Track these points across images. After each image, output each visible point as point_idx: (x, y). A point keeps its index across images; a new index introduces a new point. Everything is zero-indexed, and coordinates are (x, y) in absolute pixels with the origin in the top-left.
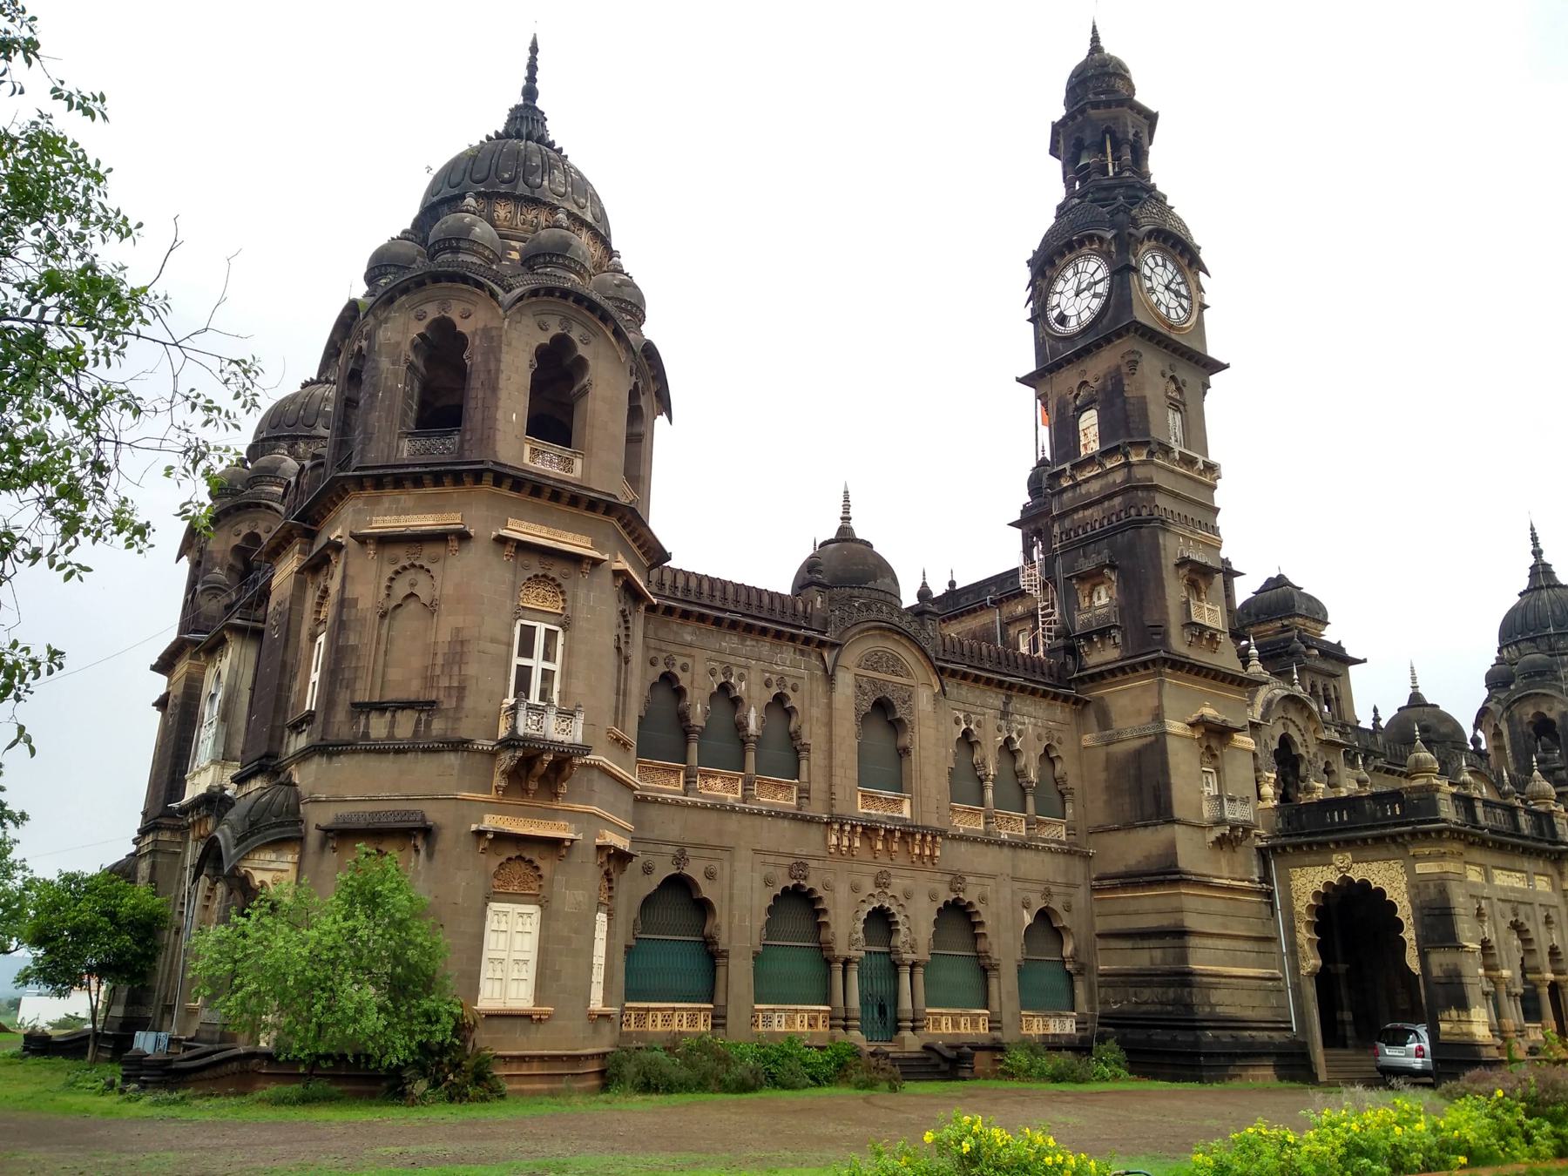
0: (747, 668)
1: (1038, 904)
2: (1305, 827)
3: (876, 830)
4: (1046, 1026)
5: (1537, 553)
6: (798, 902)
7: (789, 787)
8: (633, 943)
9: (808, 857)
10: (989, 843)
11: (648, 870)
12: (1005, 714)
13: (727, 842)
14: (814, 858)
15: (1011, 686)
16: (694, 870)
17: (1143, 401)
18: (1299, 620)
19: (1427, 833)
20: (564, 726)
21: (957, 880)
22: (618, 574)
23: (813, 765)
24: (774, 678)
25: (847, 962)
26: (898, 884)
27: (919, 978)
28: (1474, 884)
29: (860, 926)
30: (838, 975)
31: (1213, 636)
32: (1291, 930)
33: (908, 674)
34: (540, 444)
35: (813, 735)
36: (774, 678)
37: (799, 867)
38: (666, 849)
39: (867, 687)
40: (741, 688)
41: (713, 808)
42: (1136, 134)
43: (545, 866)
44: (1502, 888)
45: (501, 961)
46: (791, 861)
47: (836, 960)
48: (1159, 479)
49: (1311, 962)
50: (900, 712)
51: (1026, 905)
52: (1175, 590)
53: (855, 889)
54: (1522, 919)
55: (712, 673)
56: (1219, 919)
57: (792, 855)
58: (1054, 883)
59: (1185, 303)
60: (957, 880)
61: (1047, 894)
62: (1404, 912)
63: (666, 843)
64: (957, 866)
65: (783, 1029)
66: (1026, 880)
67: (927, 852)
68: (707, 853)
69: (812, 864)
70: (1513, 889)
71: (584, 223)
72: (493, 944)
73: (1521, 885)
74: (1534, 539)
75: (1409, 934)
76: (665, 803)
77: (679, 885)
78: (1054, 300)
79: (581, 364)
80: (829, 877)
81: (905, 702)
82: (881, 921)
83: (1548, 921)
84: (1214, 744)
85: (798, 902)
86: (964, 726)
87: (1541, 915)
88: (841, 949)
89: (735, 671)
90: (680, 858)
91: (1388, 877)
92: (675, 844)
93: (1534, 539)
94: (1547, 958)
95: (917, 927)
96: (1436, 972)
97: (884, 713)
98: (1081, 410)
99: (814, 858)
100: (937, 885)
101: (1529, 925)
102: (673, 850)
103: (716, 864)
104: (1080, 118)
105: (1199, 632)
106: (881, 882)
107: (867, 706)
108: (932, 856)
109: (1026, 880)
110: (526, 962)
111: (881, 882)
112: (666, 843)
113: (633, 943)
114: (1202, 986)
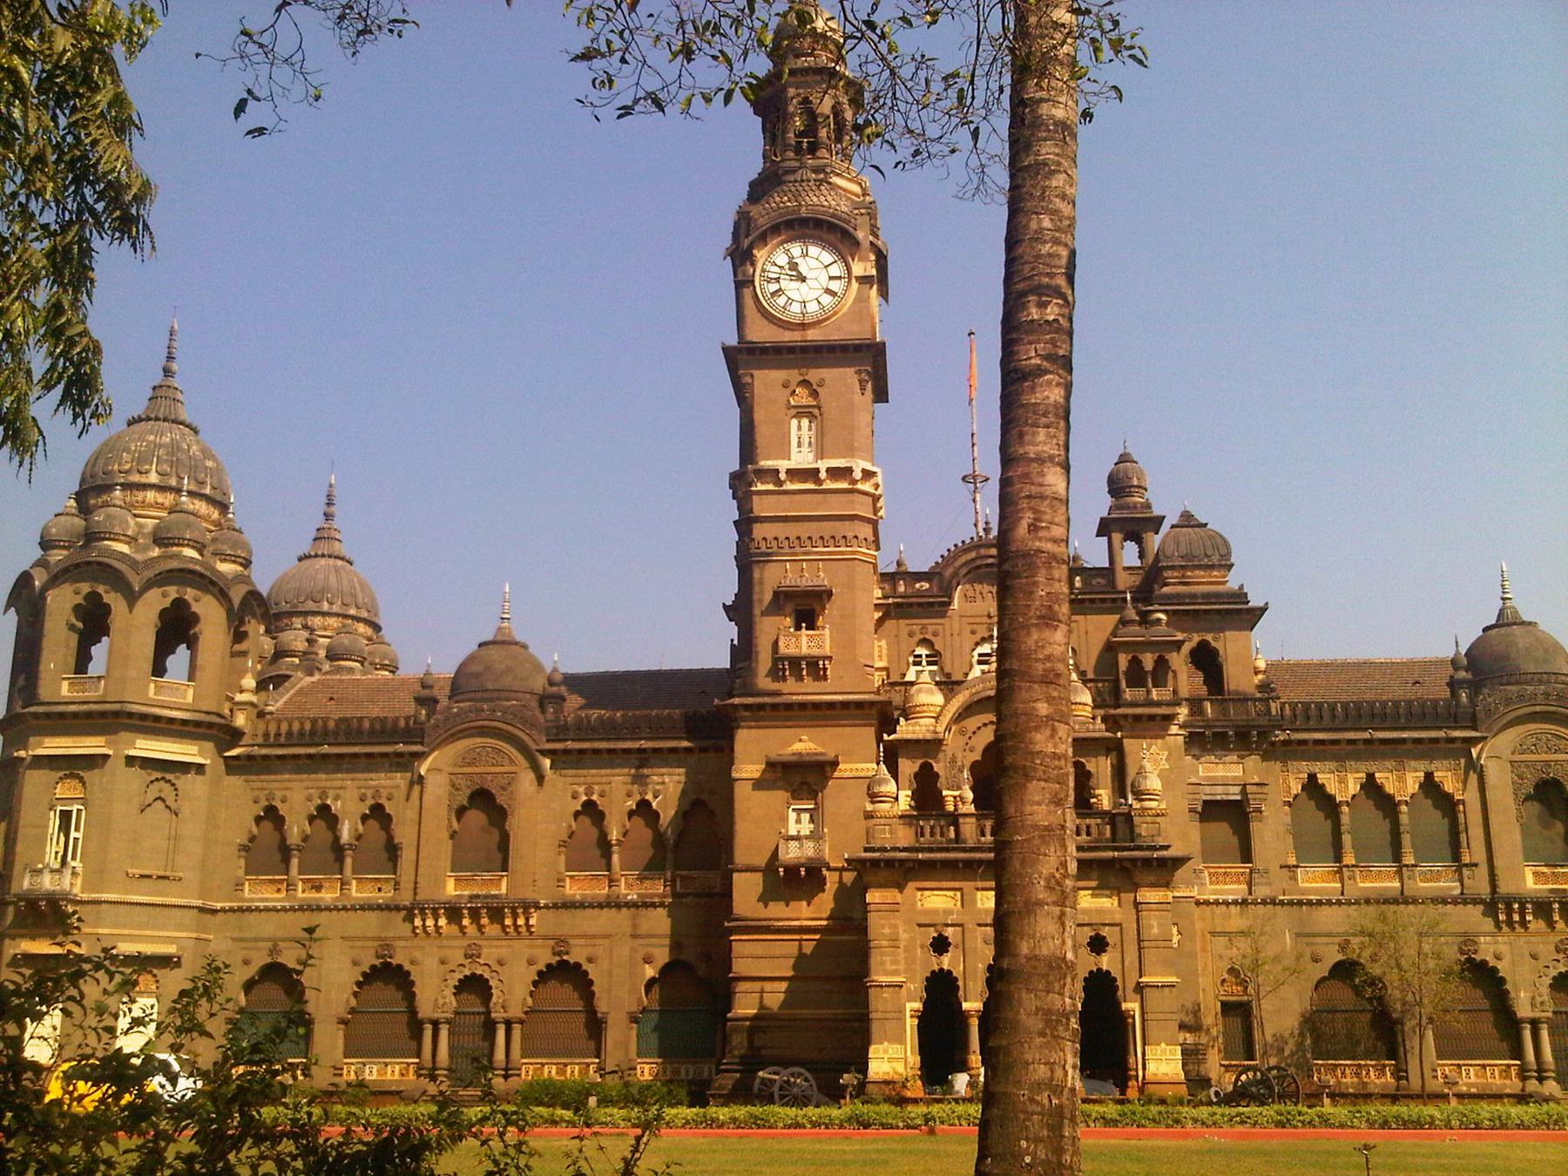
6: (388, 975)
9: (394, 938)
14: (401, 938)
15: (641, 751)
24: (369, 793)
26: (489, 953)
35: (404, 834)
37: (386, 947)
38: (261, 944)
39: (462, 782)
40: (336, 807)
41: (301, 909)
46: (376, 944)
50: (501, 800)
51: (648, 960)
53: (443, 962)
55: (309, 799)
57: (379, 939)
60: (561, 944)
64: (564, 931)
65: (374, 1077)
76: (258, 909)
80: (417, 954)
82: (474, 986)
84: (810, 780)
85: (388, 975)
89: (331, 793)
90: (274, 951)
92: (269, 940)
95: (513, 990)
97: (485, 803)
99: (401, 938)
107: (462, 799)
108: (528, 926)
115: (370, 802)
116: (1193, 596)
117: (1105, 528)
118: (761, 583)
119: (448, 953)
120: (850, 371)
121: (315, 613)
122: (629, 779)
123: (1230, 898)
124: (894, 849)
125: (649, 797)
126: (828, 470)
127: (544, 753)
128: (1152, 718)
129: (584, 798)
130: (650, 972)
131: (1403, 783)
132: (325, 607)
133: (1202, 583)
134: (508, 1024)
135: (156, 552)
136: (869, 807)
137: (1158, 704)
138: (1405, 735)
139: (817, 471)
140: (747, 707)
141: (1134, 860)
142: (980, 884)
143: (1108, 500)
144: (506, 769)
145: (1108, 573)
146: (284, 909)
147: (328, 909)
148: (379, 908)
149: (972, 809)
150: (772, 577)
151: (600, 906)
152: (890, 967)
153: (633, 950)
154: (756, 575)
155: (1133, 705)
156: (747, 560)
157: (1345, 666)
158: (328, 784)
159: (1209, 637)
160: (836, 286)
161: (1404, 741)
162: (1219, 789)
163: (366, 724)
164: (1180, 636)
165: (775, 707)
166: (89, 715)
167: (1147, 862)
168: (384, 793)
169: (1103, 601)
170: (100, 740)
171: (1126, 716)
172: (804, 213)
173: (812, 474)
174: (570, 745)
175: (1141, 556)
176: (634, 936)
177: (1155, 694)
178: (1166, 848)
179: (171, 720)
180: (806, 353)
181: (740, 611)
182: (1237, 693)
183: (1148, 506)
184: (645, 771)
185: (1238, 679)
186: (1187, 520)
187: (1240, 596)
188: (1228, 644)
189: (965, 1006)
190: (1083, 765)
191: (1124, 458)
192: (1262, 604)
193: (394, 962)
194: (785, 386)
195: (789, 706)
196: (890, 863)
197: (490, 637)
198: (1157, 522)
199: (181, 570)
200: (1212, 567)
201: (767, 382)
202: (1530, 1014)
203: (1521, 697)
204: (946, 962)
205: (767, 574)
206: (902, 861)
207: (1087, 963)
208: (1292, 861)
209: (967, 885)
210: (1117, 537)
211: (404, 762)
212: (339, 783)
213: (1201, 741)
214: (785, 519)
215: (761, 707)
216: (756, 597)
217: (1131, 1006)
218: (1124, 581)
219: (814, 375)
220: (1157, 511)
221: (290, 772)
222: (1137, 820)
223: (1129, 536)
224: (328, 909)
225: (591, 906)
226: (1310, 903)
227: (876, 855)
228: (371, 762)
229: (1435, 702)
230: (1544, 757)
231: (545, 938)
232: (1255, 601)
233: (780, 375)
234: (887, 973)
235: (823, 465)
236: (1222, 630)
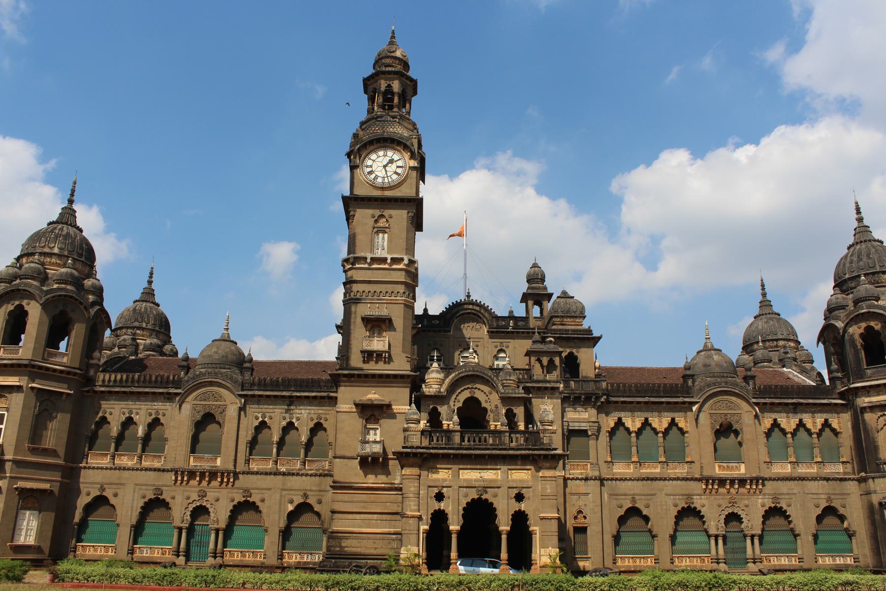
4: (303, 558)
7: (160, 457)
10: (275, 474)
11: (88, 494)
12: (287, 411)
13: (123, 481)
16: (108, 493)
24: (153, 412)
26: (211, 495)
30: (713, 542)
36: (153, 412)
37: (159, 491)
40: (136, 418)
51: (291, 502)
56: (362, 504)
58: (311, 490)
60: (247, 492)
61: (306, 496)
63: (96, 483)
64: (248, 485)
69: (164, 488)
76: (94, 468)
81: (221, 413)
84: (376, 413)
89: (134, 411)
90: (102, 489)
102: (99, 486)
103: (118, 491)
106: (203, 495)
111: (203, 495)
112: (96, 483)
115: (154, 416)
116: (566, 330)
117: (525, 298)
118: (355, 313)
120: (405, 212)
121: (139, 328)
122: (284, 411)
123: (580, 477)
124: (418, 447)
125: (294, 420)
126: (392, 259)
127: (240, 396)
128: (546, 388)
129: (261, 419)
130: (291, 508)
131: (660, 422)
132: (144, 325)
133: (570, 325)
134: (217, 531)
135: (55, 286)
136: (406, 426)
137: (549, 382)
138: (663, 400)
139: (386, 259)
140: (345, 375)
141: (539, 455)
142: (461, 467)
143: (527, 285)
145: (526, 319)
146: (107, 469)
147: (129, 469)
148: (155, 470)
149: (458, 428)
150: (364, 310)
151: (266, 474)
152: (413, 508)
153: (281, 496)
154: (353, 309)
155: (538, 381)
156: (349, 302)
157: (631, 370)
158: (133, 407)
159: (574, 351)
160: (399, 171)
161: (662, 403)
162: (576, 424)
164: (561, 349)
165: (359, 376)
166: (12, 365)
167: (546, 456)
168: (161, 412)
169: (523, 333)
170: (16, 379)
171: (533, 387)
172: (386, 135)
173: (383, 260)
174: (257, 393)
175: (541, 312)
177: (548, 377)
178: (556, 449)
179: (55, 370)
180: (382, 201)
181: (344, 328)
182: (586, 377)
183: (545, 288)
185: (586, 370)
186: (565, 295)
187: (589, 331)
188: (583, 354)
189: (451, 528)
190: (512, 410)
191: (535, 266)
192: (599, 335)
193: (161, 497)
194: (373, 217)
195: (366, 376)
196: (415, 455)
197: (218, 337)
198: (550, 296)
199: (65, 296)
200: (576, 317)
201: (364, 216)
202: (716, 533)
203: (714, 384)
204: (442, 505)
205: (358, 309)
206: (422, 454)
207: (515, 506)
208: (609, 459)
209: (455, 467)
210: (530, 303)
211: (169, 397)
212: (138, 407)
213: (571, 400)
214: (369, 282)
215: (352, 376)
216: (352, 320)
217: (535, 528)
218: (532, 323)
219: (387, 213)
220: (550, 291)
221: (115, 400)
222: (542, 435)
223: (535, 303)
224: (129, 469)
225: (261, 474)
226: (616, 479)
227: (409, 450)
228: (155, 397)
229: (677, 385)
230: (726, 412)
231: (238, 489)
232: (596, 334)
233: (370, 212)
234: (411, 511)
235: (389, 257)
236: (580, 347)
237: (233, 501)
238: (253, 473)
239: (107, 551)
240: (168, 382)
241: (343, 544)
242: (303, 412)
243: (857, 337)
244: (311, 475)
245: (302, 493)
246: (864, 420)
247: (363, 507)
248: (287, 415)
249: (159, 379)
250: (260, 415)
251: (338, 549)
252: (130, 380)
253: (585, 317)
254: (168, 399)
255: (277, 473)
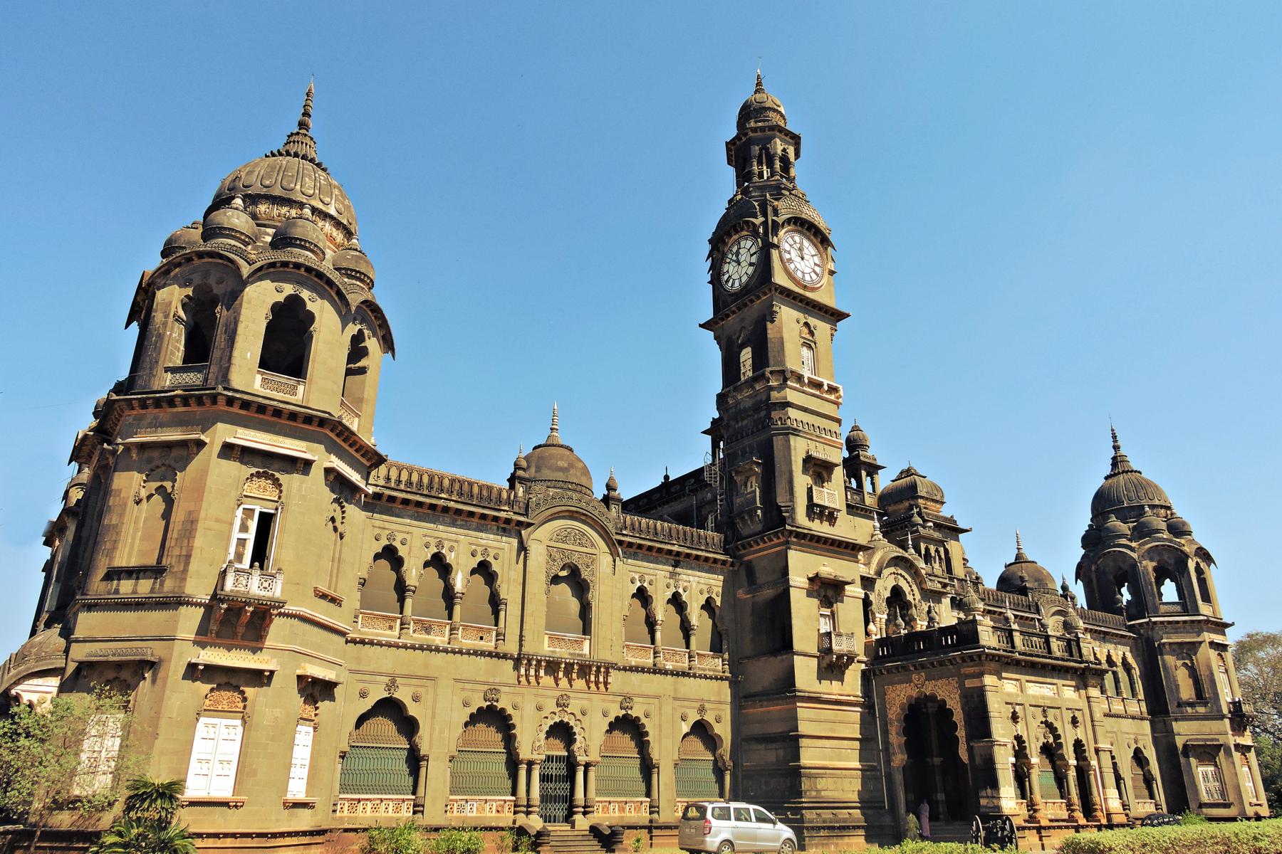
0: (457, 541)
1: (694, 717)
2: (893, 655)
3: (559, 664)
5: (1116, 448)
8: (348, 749)
12: (673, 575)
13: (431, 674)
16: (403, 695)
17: (781, 342)
18: (920, 501)
19: (971, 657)
20: (266, 584)
21: (626, 700)
22: (328, 471)
23: (511, 613)
24: (479, 550)
25: (530, 764)
26: (575, 705)
27: (592, 775)
28: (1009, 695)
29: (543, 735)
31: (831, 514)
32: (886, 733)
33: (593, 545)
34: (271, 375)
40: (450, 558)
42: (784, 150)
43: (250, 691)
44: (1034, 697)
45: (208, 761)
46: (487, 687)
47: (521, 762)
48: (791, 396)
49: (899, 759)
50: (585, 574)
52: (802, 481)
53: (539, 709)
54: (1050, 719)
58: (709, 701)
59: (817, 269)
60: (626, 700)
61: (702, 710)
62: (958, 717)
63: (380, 674)
64: (628, 690)
66: (685, 700)
67: (601, 679)
68: (414, 681)
69: (503, 689)
70: (1043, 698)
71: (326, 216)
72: (200, 748)
73: (1051, 694)
74: (1114, 437)
75: (961, 733)
77: (389, 708)
78: (726, 267)
79: (311, 317)
80: (518, 700)
81: (588, 566)
82: (562, 732)
83: (1074, 721)
86: (639, 584)
87: (1068, 716)
88: (525, 753)
89: (447, 545)
90: (392, 685)
91: (949, 694)
93: (1114, 437)
94: (1071, 749)
95: (592, 739)
96: (978, 760)
98: (742, 346)
100: (610, 705)
101: (1057, 724)
102: (386, 679)
103: (422, 691)
104: (744, 139)
105: (816, 511)
106: (562, 704)
109: (685, 700)
110: (229, 762)
111: (562, 704)
112: (380, 674)
113: (348, 749)
114: (810, 776)
119: (541, 700)
122: (668, 574)
144: (588, 550)
146: (389, 645)
148: (482, 654)
158: (444, 535)
163: (476, 490)
168: (492, 552)
176: (675, 699)
184: (678, 570)
212: (453, 536)
221: (411, 517)
237: (647, 716)
238: (665, 672)
239: (397, 810)
240: (500, 501)
241: (819, 787)
242: (691, 578)
243: (1150, 569)
244: (711, 678)
245: (697, 705)
246: (1163, 661)
247: (833, 730)
248: (672, 581)
249: (485, 493)
250: (637, 577)
251: (814, 794)
252: (436, 486)
253: (943, 503)
254: (504, 530)
255: (656, 670)
